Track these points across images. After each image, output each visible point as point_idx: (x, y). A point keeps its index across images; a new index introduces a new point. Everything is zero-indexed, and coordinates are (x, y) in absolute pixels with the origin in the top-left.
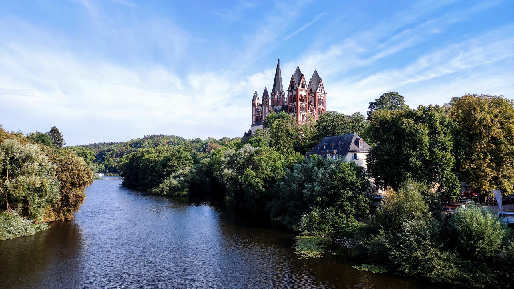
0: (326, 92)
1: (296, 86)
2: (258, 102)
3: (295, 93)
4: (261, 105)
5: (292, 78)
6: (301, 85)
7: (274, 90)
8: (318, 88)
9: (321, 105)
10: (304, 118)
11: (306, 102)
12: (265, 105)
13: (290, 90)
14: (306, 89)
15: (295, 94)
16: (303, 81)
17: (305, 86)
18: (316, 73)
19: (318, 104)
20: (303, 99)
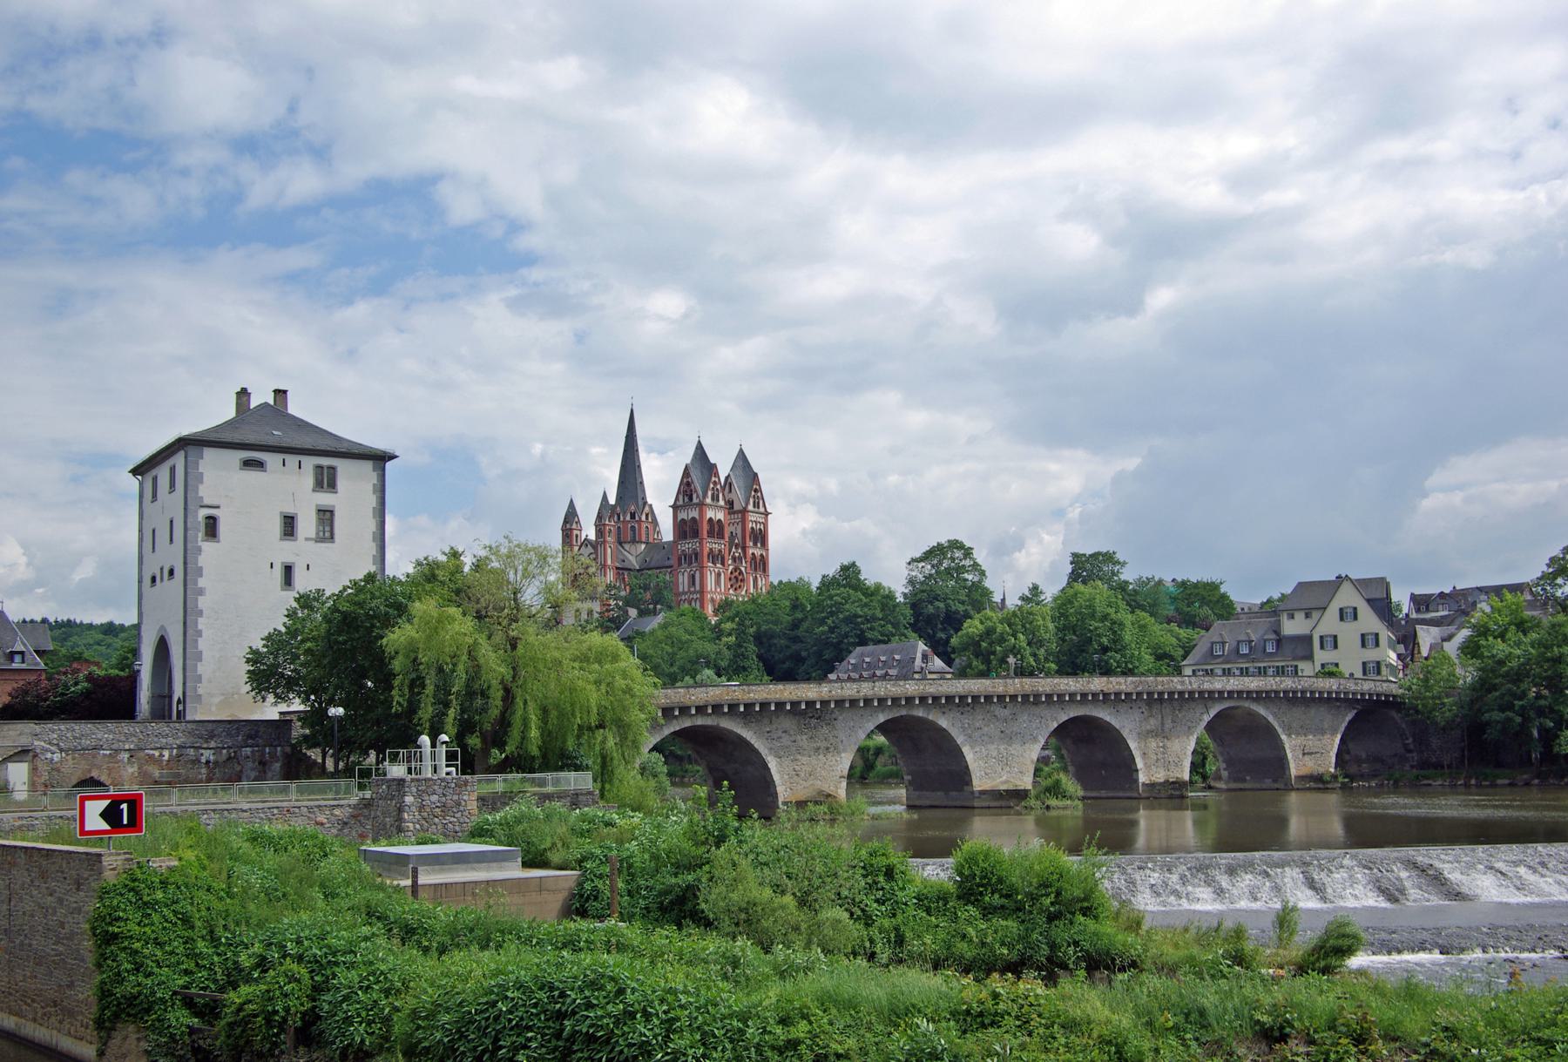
0: (769, 510)
1: (698, 497)
2: (578, 532)
3: (694, 514)
4: (594, 545)
5: (686, 472)
6: (710, 493)
7: (620, 497)
8: (751, 501)
9: (759, 545)
10: (718, 582)
11: (723, 538)
12: (605, 542)
13: (681, 506)
14: (722, 503)
15: (693, 518)
16: (715, 483)
17: (721, 495)
18: (741, 456)
19: (751, 544)
20: (716, 529)
